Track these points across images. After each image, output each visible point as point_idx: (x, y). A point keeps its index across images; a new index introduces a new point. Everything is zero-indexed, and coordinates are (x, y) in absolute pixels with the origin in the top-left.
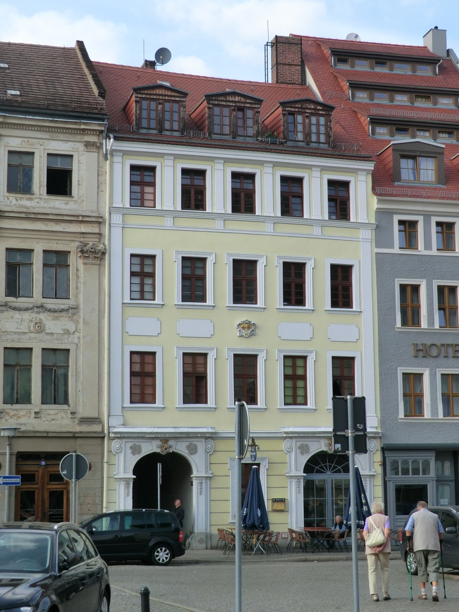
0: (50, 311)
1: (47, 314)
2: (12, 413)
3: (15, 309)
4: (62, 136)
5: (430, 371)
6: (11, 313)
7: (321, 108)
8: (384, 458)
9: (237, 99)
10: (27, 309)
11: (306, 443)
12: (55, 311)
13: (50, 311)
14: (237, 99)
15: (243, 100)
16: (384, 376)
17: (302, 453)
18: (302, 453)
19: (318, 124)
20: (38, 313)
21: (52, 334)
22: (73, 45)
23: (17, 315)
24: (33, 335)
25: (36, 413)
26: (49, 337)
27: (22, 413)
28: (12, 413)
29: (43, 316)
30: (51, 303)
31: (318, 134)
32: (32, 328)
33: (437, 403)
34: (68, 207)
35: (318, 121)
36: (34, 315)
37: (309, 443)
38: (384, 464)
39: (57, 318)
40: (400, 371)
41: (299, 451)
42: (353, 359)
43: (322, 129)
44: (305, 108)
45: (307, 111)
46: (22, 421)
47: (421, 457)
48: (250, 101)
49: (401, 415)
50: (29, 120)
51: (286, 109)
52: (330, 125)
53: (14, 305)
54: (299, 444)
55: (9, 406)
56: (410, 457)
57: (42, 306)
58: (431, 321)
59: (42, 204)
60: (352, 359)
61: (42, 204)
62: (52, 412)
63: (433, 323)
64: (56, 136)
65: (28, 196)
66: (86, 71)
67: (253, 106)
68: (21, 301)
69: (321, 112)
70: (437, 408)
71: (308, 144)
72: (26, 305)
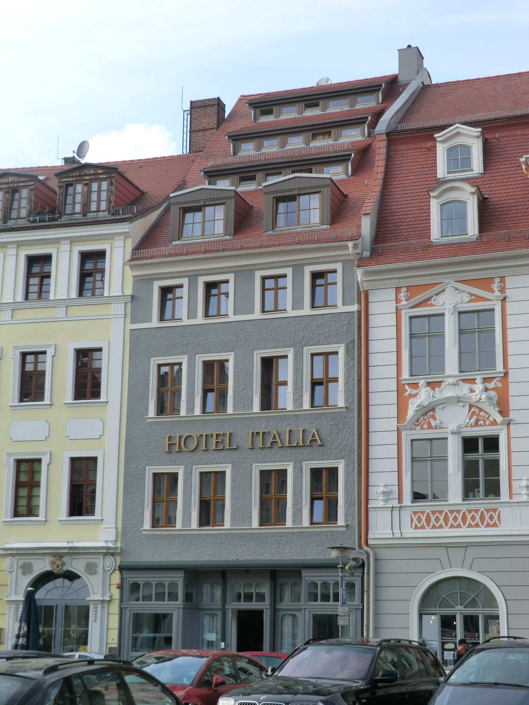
5: (185, 469)
7: (101, 172)
8: (122, 579)
9: (10, 179)
11: (30, 561)
14: (10, 179)
15: (16, 179)
16: (129, 478)
17: (24, 573)
18: (24, 573)
19: (99, 191)
31: (99, 201)
33: (190, 509)
35: (99, 187)
37: (33, 562)
38: (120, 587)
40: (150, 470)
41: (20, 571)
42: (94, 460)
43: (94, 197)
44: (83, 176)
45: (87, 178)
47: (167, 578)
48: (25, 179)
49: (147, 524)
51: (63, 180)
52: (112, 189)
54: (21, 562)
56: (154, 578)
58: (191, 408)
60: (94, 460)
63: (193, 408)
67: (27, 184)
69: (101, 176)
70: (190, 516)
71: (85, 215)
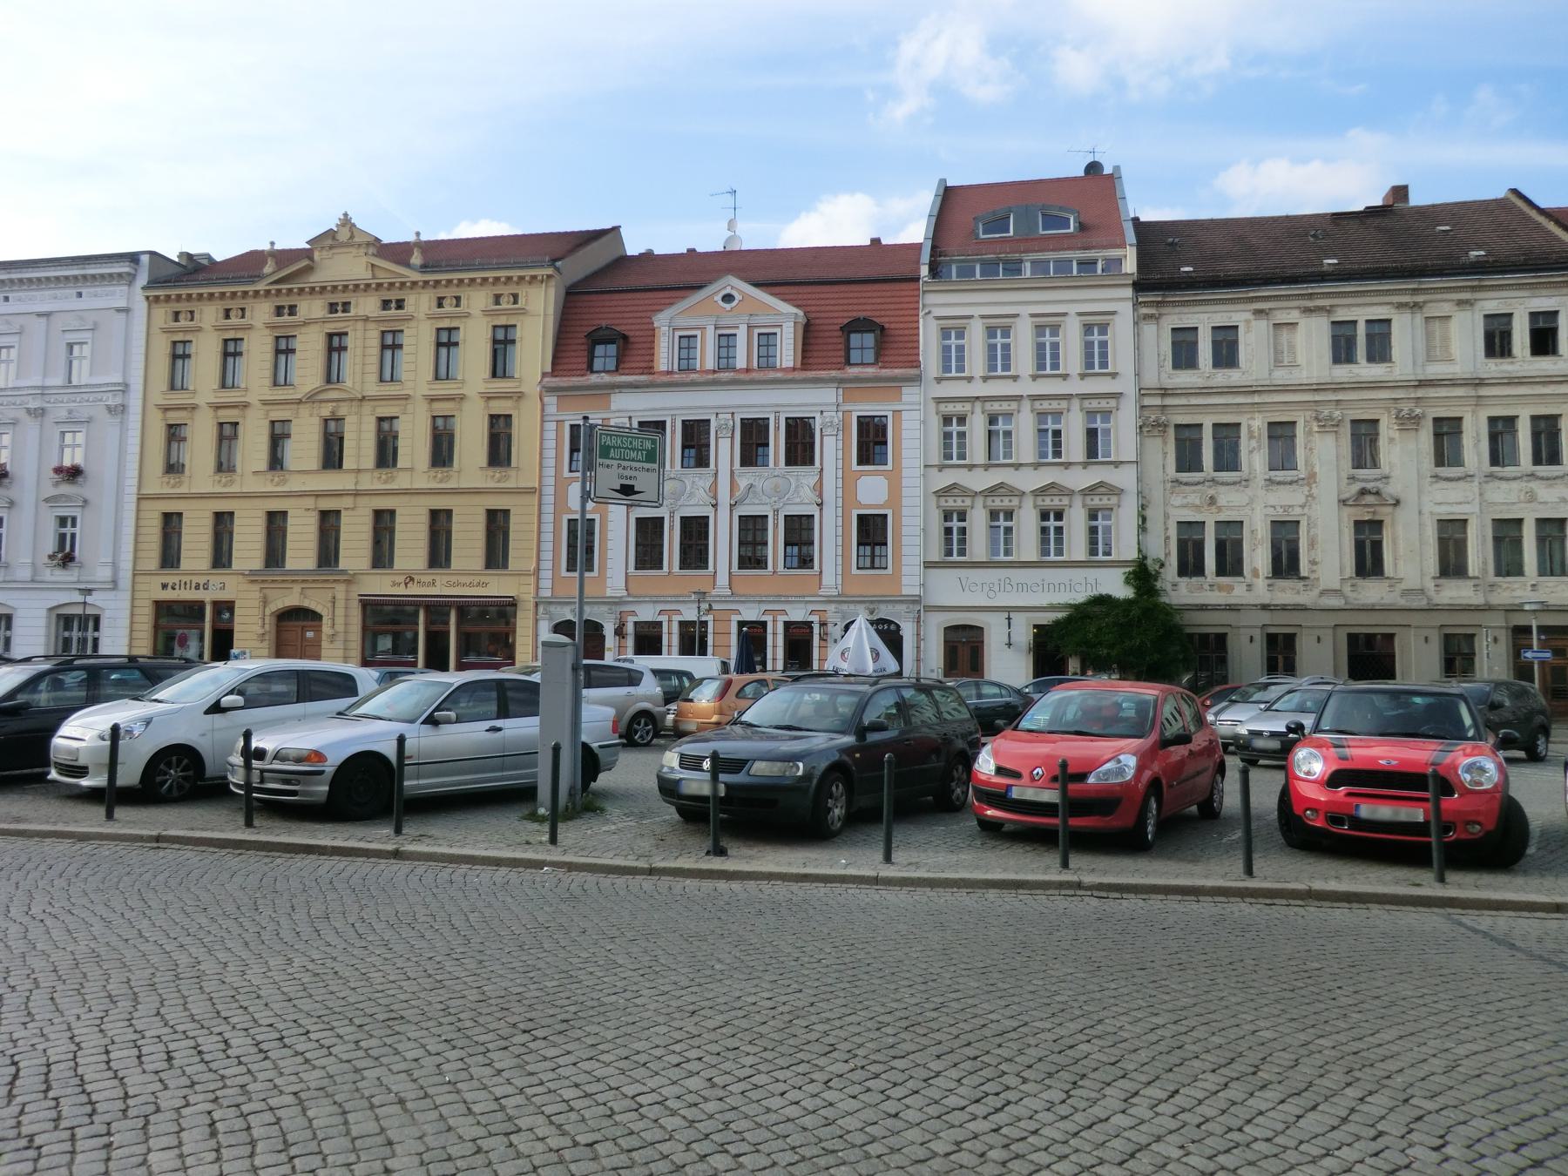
0: (1542, 478)
1: (1538, 482)
2: (1505, 586)
3: (1501, 479)
4: (1544, 292)
6: (1497, 483)
10: (1515, 479)
12: (1548, 479)
13: (1542, 478)
20: (1529, 481)
21: (1546, 503)
22: (1499, 192)
23: (1504, 485)
24: (1523, 505)
25: (1533, 585)
26: (1541, 506)
27: (1516, 586)
28: (1505, 586)
29: (1534, 485)
30: (1543, 470)
32: (1522, 498)
34: (1556, 367)
36: (1524, 484)
39: (1551, 485)
46: (1517, 594)
50: (1510, 279)
53: (1500, 475)
55: (1500, 579)
57: (1532, 475)
59: (1526, 367)
61: (1526, 367)
62: (1550, 584)
64: (1537, 292)
65: (1510, 360)
66: (1541, 219)
68: (1509, 471)
72: (1514, 475)
